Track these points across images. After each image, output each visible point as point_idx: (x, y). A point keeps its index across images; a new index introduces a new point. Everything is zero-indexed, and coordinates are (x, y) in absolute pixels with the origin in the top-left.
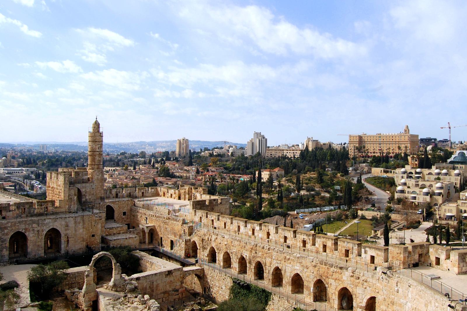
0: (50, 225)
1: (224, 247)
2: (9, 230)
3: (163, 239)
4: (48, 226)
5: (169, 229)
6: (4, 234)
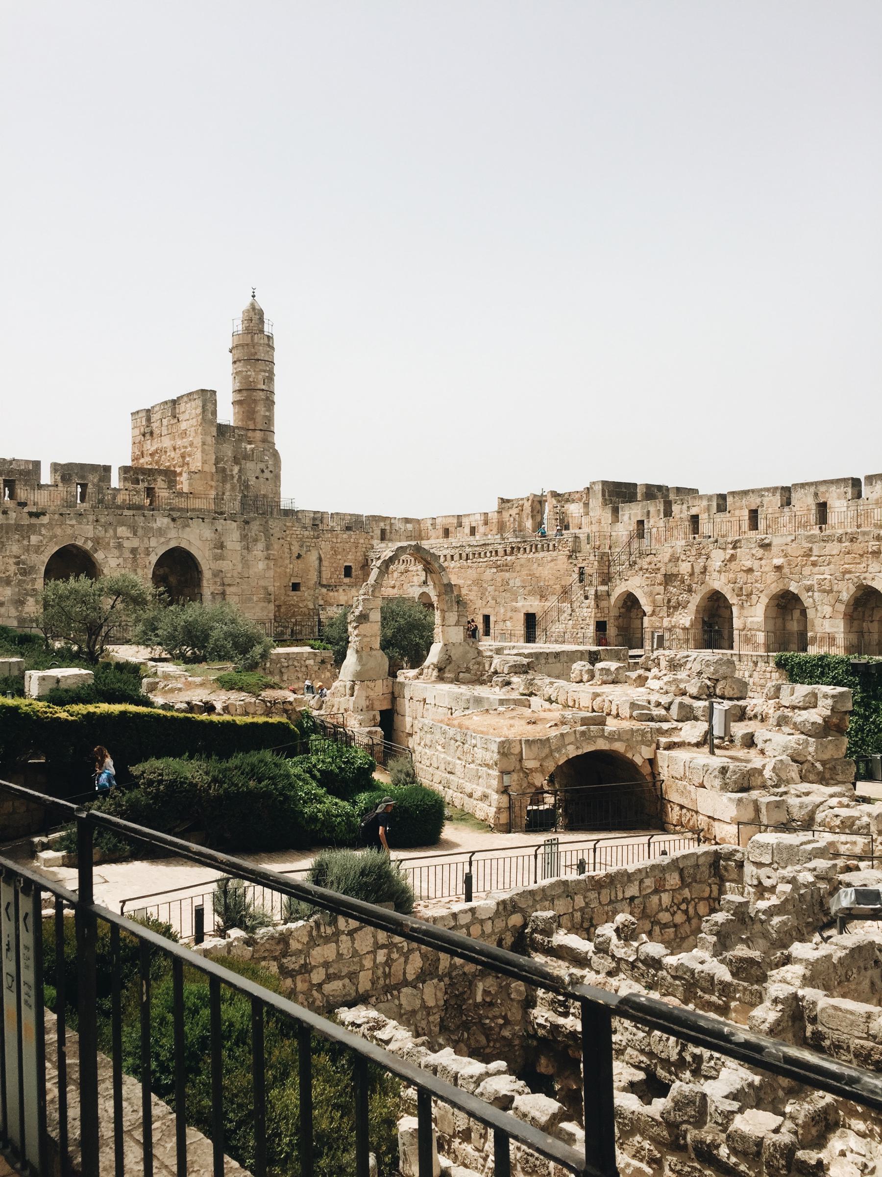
0: (169, 536)
1: (772, 576)
2: (40, 534)
3: (492, 619)
4: (163, 540)
5: (516, 581)
6: (27, 549)
